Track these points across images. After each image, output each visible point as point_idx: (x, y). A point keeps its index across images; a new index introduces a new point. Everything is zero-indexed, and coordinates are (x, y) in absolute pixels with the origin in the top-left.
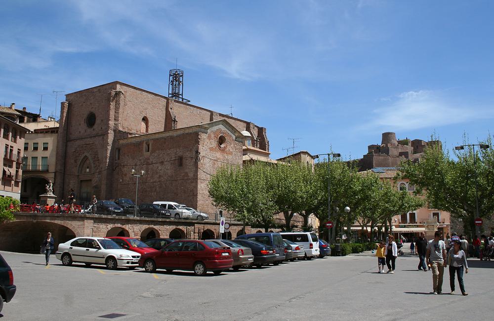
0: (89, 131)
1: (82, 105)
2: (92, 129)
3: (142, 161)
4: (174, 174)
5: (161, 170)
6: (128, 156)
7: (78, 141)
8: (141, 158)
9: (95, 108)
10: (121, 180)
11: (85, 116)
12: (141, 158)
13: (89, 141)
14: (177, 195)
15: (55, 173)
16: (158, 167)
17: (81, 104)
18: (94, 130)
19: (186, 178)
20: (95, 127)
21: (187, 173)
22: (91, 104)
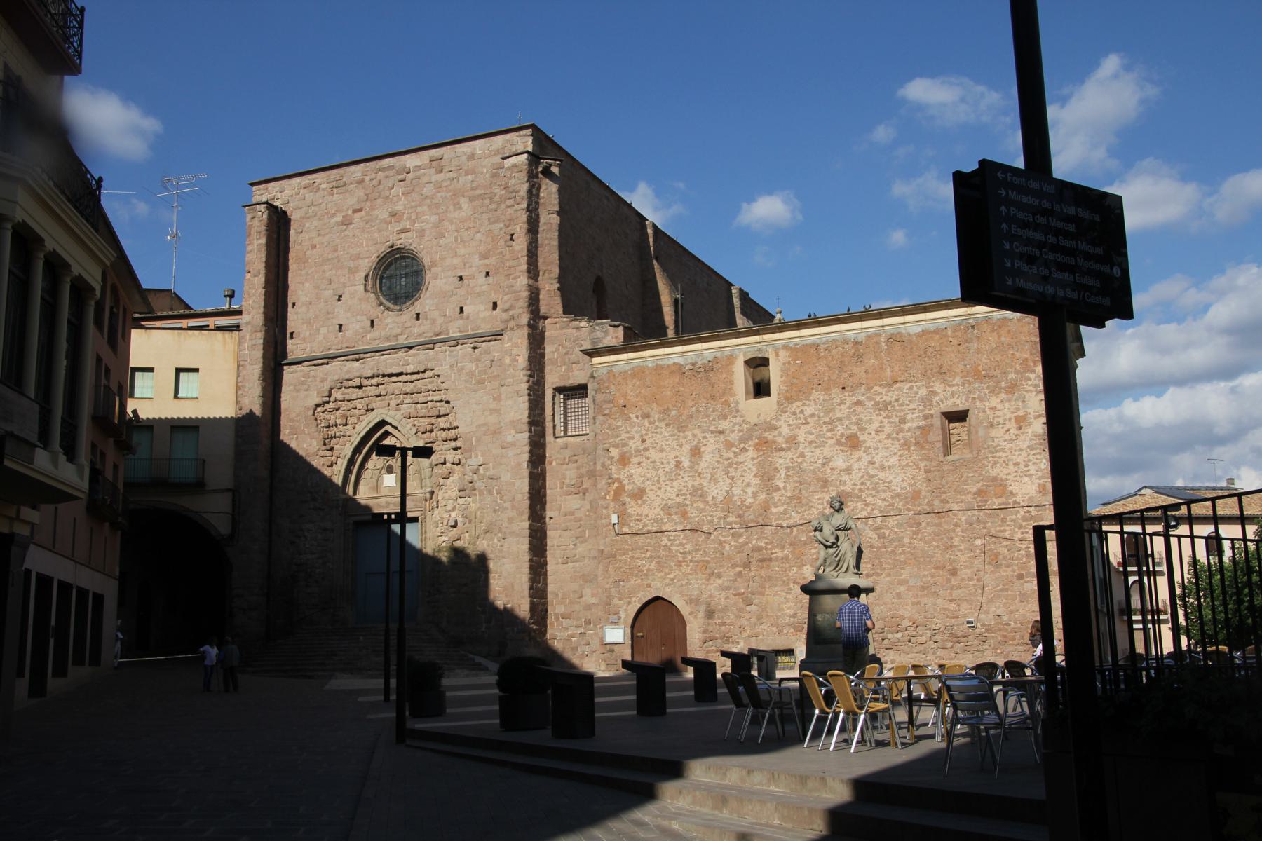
0: (395, 323)
1: (347, 222)
2: (409, 313)
3: (733, 437)
4: (924, 488)
5: (848, 470)
6: (646, 416)
7: (335, 364)
8: (723, 425)
9: (421, 233)
10: (614, 519)
11: (367, 264)
12: (723, 425)
13: (413, 360)
14: (954, 572)
15: (234, 491)
16: (827, 460)
17: (339, 218)
18: (418, 316)
19: (996, 502)
20: (425, 302)
21: (1000, 485)
22: (393, 214)
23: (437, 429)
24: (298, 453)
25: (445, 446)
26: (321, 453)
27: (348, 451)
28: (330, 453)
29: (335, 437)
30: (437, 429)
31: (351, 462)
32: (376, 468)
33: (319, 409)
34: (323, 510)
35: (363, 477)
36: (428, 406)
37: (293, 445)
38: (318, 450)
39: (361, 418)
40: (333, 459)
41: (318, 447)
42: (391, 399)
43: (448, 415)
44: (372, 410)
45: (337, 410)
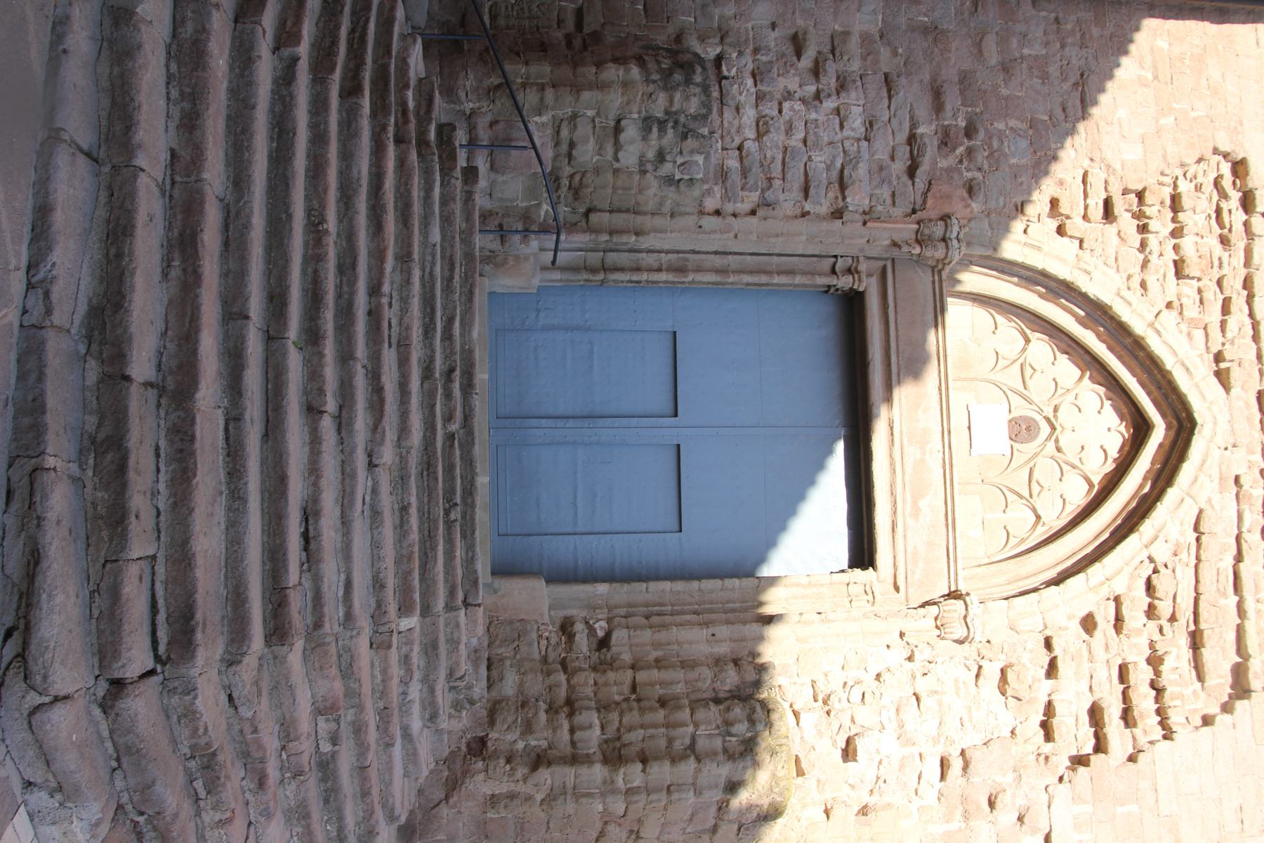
23: (1156, 637)
24: (1102, 90)
25: (1105, 673)
26: (1096, 180)
27: (1099, 286)
28: (1097, 211)
29: (1143, 229)
30: (1156, 637)
31: (1061, 290)
32: (1028, 371)
33: (1226, 168)
34: (912, 172)
35: (999, 319)
36: (1224, 595)
37: (1127, 69)
38: (1108, 167)
39: (1199, 335)
40: (1076, 225)
41: (1118, 166)
42: (1251, 452)
43: (1200, 678)
44: (1226, 386)
45: (1224, 241)
